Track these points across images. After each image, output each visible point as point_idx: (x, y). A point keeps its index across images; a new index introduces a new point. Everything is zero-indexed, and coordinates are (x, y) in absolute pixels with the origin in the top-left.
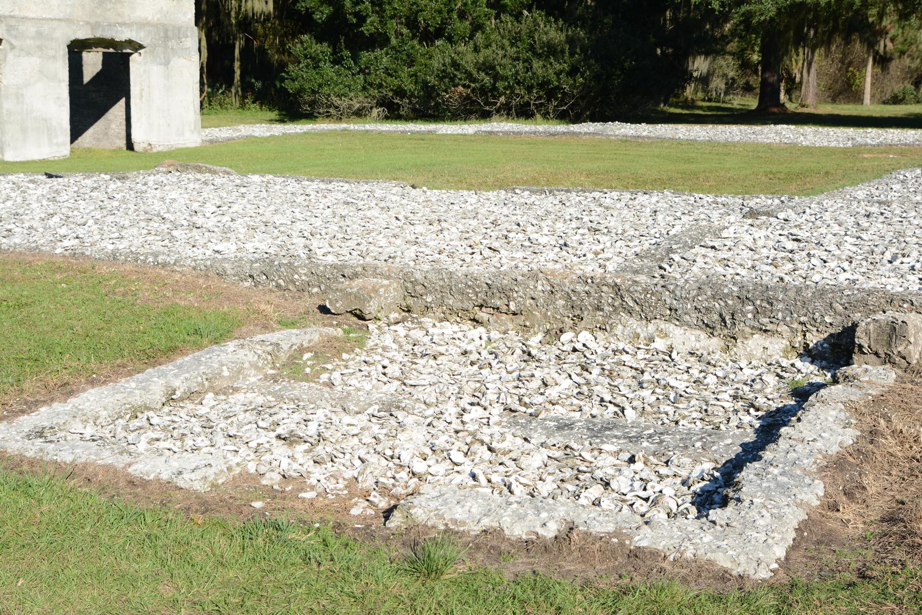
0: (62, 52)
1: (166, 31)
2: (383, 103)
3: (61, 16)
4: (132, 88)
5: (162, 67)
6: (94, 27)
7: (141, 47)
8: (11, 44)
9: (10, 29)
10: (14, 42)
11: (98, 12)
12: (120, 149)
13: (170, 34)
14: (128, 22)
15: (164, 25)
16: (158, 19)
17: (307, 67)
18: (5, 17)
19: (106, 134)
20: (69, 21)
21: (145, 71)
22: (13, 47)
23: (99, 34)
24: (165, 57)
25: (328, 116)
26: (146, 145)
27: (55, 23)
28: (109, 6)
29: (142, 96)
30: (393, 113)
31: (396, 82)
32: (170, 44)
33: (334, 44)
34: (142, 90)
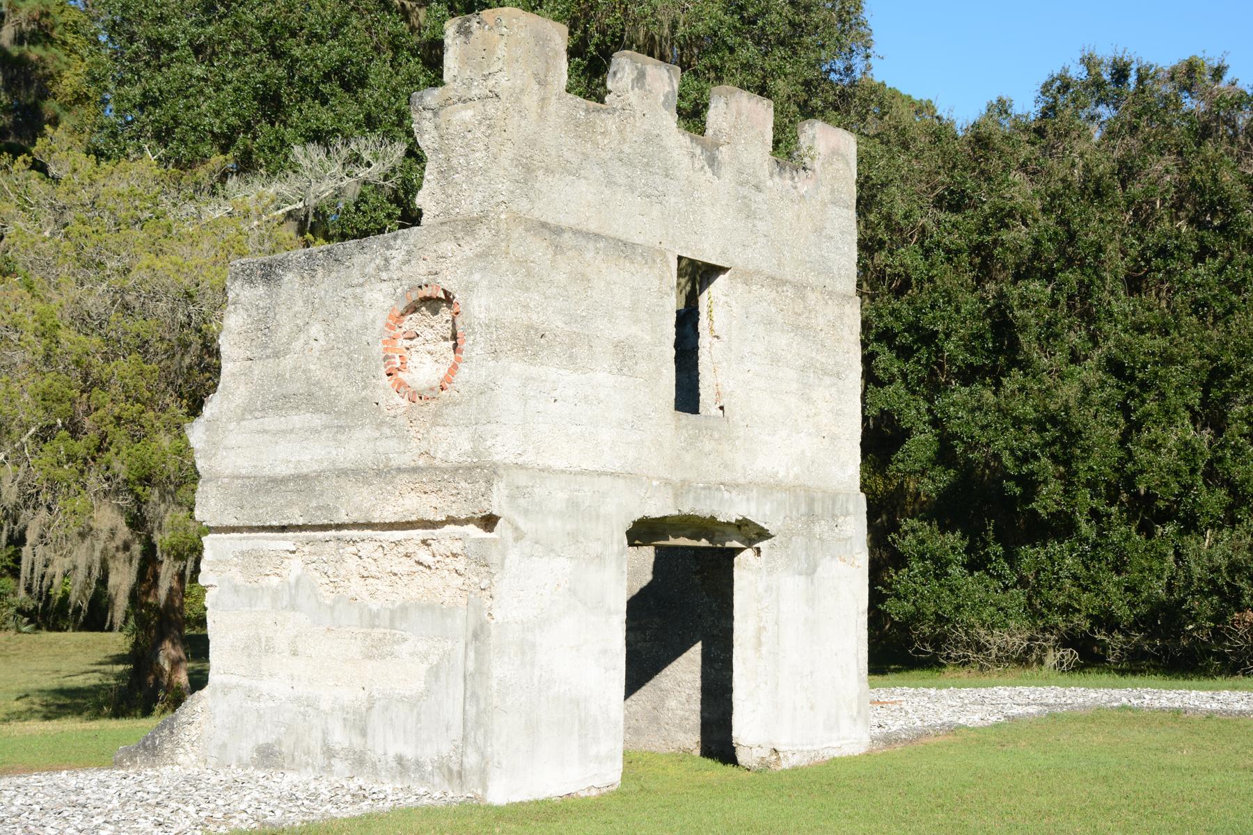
0: (616, 547)
1: (811, 502)
2: (1069, 640)
3: (617, 466)
4: (737, 625)
5: (803, 578)
6: (681, 488)
7: (763, 534)
8: (516, 529)
9: (516, 493)
10: (521, 522)
11: (688, 457)
12: (687, 752)
13: (818, 508)
14: (741, 481)
15: (807, 489)
16: (797, 477)
17: (923, 574)
18: (507, 467)
19: (655, 720)
20: (630, 476)
21: (768, 589)
22: (519, 536)
23: (688, 507)
24: (808, 556)
25: (964, 664)
26: (765, 753)
27: (605, 482)
28: (708, 446)
29: (759, 643)
30: (1088, 656)
31: (1097, 602)
32: (817, 529)
33: (974, 533)
34: (761, 630)
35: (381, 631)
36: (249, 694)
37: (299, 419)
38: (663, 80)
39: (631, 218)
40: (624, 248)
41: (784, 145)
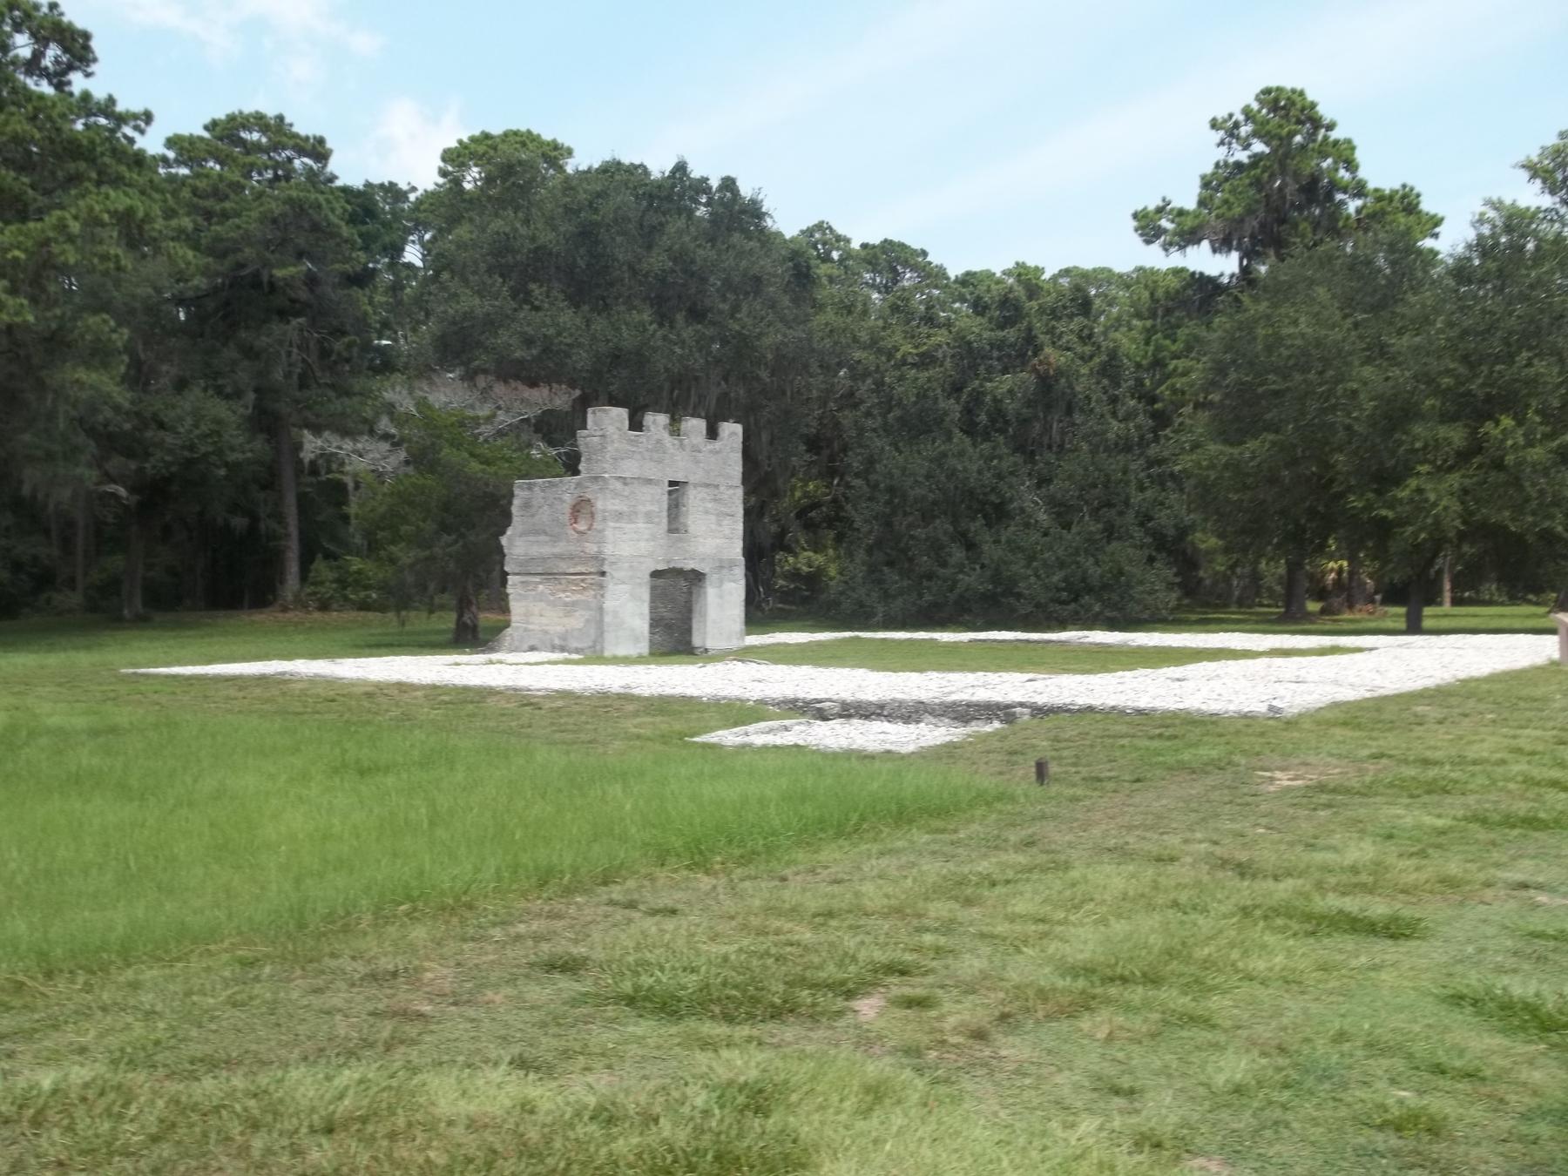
35: (570, 608)
36: (526, 630)
37: (542, 538)
38: (662, 419)
39: (651, 471)
40: (649, 481)
41: (712, 434)
